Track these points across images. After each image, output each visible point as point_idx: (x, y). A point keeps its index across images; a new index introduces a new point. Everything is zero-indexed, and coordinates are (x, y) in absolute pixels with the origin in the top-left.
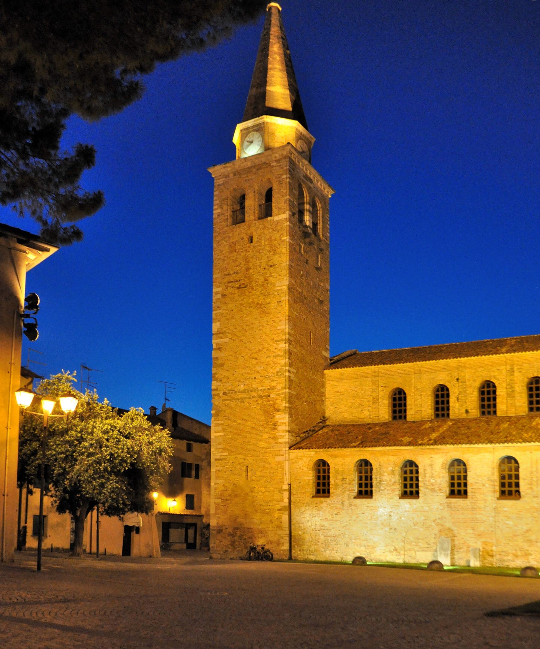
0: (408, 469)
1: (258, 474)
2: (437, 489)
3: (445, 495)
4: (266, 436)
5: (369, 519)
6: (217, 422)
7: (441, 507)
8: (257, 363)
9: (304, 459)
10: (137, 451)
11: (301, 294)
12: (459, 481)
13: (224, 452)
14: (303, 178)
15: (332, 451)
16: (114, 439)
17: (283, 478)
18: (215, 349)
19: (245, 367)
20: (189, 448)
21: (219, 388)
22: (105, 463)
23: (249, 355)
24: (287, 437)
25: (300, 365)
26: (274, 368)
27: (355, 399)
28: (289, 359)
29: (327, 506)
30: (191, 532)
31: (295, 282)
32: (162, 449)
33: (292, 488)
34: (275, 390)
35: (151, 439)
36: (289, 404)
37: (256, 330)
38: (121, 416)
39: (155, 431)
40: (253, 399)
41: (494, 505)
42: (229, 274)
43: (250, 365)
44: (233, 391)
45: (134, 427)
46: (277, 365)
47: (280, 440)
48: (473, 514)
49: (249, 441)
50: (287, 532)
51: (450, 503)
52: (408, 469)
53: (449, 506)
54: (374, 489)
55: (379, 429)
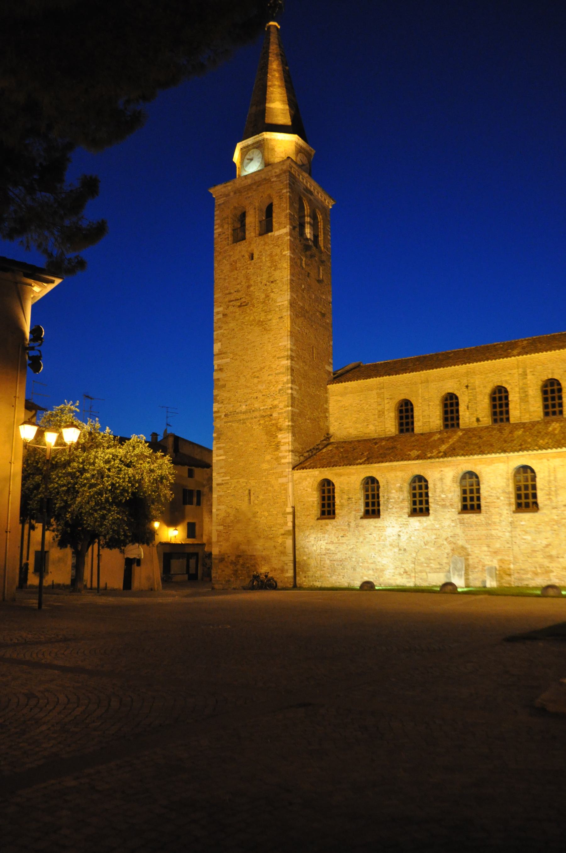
0: (417, 484)
1: (261, 497)
2: (448, 504)
3: (457, 510)
4: (268, 457)
5: (377, 540)
6: (219, 445)
7: (453, 524)
8: (259, 382)
9: (308, 479)
10: (138, 479)
11: (302, 308)
12: (472, 495)
13: (226, 476)
14: (303, 191)
15: (337, 469)
16: (116, 469)
17: (287, 501)
18: (217, 370)
19: (247, 387)
20: (191, 474)
21: (220, 410)
22: (106, 494)
23: (250, 374)
24: (290, 457)
25: (303, 381)
26: (276, 386)
27: (360, 414)
28: (292, 375)
29: (332, 529)
30: (192, 562)
31: (297, 296)
32: (164, 476)
33: (296, 511)
34: (277, 409)
35: (152, 466)
36: (292, 422)
37: (258, 348)
38: (123, 445)
39: (157, 458)
40: (255, 420)
41: (510, 519)
42: (230, 293)
43: (252, 384)
44: (235, 413)
45: (135, 455)
46: (279, 382)
47: (283, 461)
48: (488, 530)
49: (251, 464)
50: (291, 558)
51: (463, 519)
52: (417, 484)
53: (462, 522)
54: (381, 508)
55: (386, 444)
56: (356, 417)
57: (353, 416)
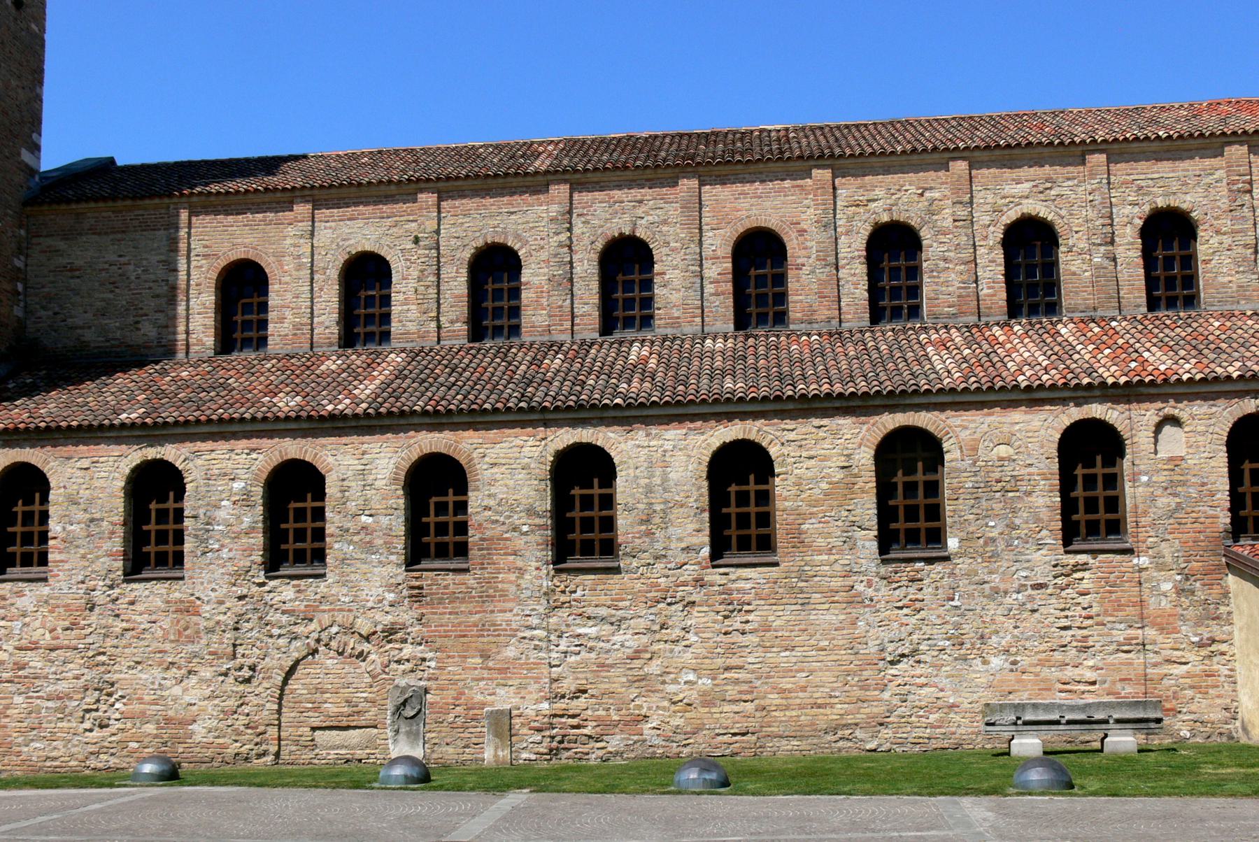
5: (172, 637)
7: (391, 597)
27: (117, 291)
56: (103, 300)
57: (97, 295)
